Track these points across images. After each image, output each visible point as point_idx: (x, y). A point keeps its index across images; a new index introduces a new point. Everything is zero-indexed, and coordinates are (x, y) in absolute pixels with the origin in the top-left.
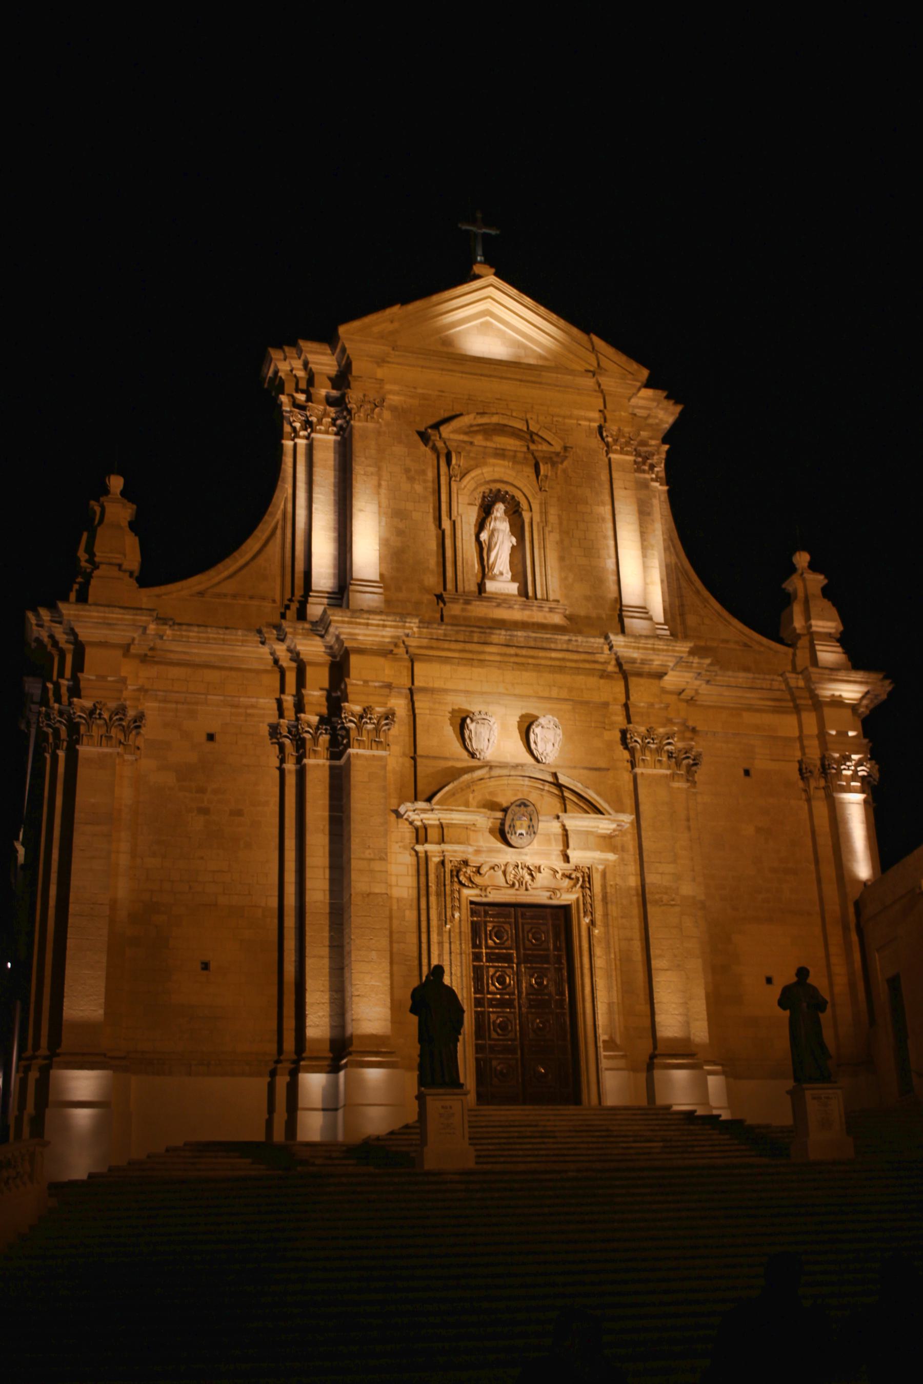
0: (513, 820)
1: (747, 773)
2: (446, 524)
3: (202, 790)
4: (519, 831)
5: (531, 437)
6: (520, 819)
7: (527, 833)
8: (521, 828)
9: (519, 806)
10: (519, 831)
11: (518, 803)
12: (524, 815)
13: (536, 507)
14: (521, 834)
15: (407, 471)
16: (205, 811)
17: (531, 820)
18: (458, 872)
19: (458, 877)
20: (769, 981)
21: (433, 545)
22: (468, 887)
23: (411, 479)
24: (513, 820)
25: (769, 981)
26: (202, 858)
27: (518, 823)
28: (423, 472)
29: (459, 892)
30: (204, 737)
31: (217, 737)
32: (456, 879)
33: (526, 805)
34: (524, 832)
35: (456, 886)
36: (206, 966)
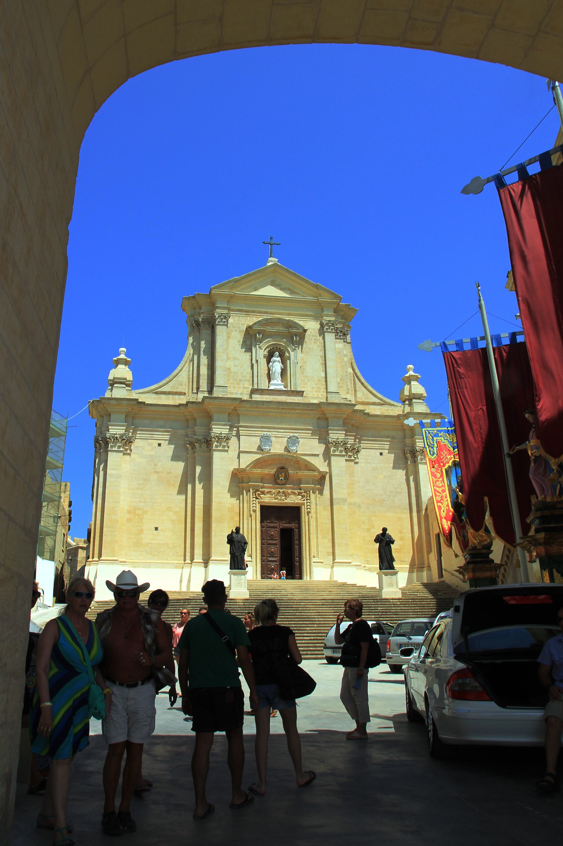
0: (278, 474)
2: (254, 362)
4: (281, 478)
6: (281, 474)
7: (284, 479)
8: (282, 477)
9: (281, 469)
10: (281, 478)
11: (280, 468)
13: (292, 354)
14: (282, 479)
17: (286, 474)
24: (278, 474)
27: (280, 475)
29: (256, 501)
34: (283, 479)
35: (255, 499)
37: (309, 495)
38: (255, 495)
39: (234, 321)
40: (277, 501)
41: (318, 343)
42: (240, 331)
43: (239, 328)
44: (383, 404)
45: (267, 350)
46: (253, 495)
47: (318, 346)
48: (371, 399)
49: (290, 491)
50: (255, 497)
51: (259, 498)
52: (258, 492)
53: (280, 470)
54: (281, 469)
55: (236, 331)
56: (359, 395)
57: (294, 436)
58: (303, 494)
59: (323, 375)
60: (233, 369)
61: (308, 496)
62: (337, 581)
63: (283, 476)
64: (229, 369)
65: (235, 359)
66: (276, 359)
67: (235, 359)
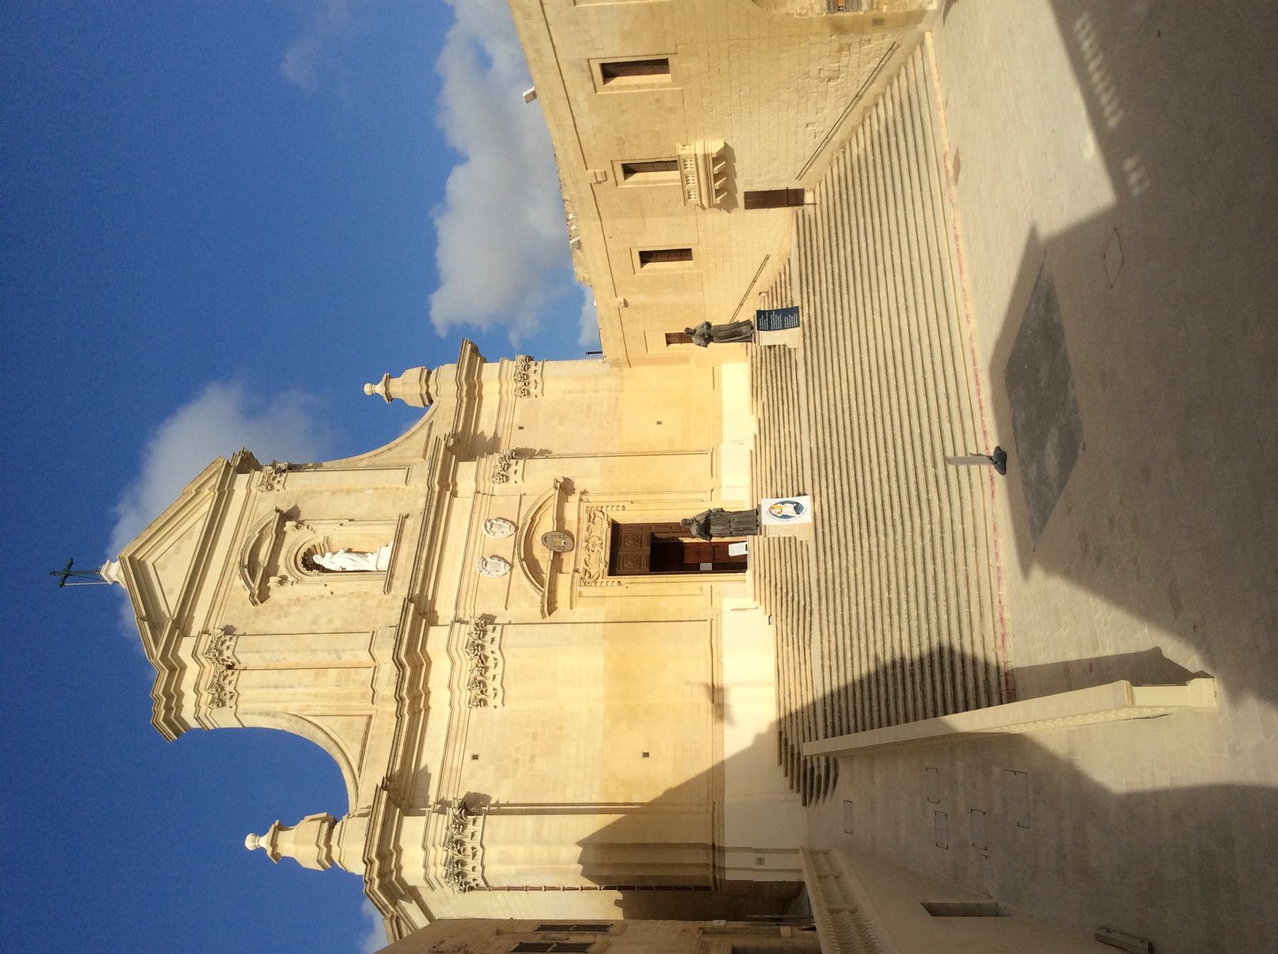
1: (521, 428)
3: (516, 761)
4: (563, 544)
6: (555, 543)
8: (561, 543)
9: (546, 542)
12: (552, 540)
15: (279, 617)
16: (533, 758)
20: (659, 423)
23: (286, 614)
25: (659, 423)
26: (567, 759)
27: (557, 544)
30: (475, 761)
31: (475, 753)
33: (546, 537)
34: (563, 541)
36: (646, 755)
40: (603, 552)
42: (257, 614)
43: (249, 617)
44: (431, 424)
45: (304, 570)
49: (584, 533)
51: (596, 577)
53: (548, 544)
54: (546, 542)
55: (253, 623)
57: (486, 526)
58: (592, 516)
59: (370, 492)
62: (756, 436)
63: (558, 539)
67: (314, 622)
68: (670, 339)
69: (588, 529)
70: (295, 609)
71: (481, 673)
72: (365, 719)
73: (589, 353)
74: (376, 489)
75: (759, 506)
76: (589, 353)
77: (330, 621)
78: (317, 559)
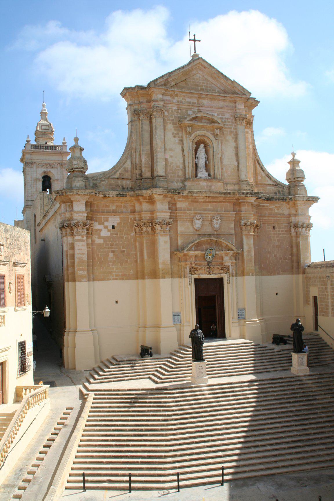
4: (209, 257)
5: (213, 122)
8: (210, 256)
14: (210, 257)
15: (173, 134)
18: (191, 270)
19: (191, 272)
21: (182, 161)
22: (194, 275)
23: (174, 137)
24: (208, 253)
27: (209, 254)
28: (178, 134)
30: (111, 228)
32: (190, 273)
34: (210, 257)
35: (190, 275)
37: (229, 269)
38: (191, 272)
39: (169, 114)
41: (233, 136)
46: (189, 272)
47: (233, 138)
48: (268, 182)
50: (191, 273)
52: (193, 269)
56: (259, 178)
58: (224, 269)
59: (236, 164)
60: (170, 160)
61: (228, 270)
64: (166, 160)
65: (171, 150)
66: (202, 150)
67: (171, 150)
68: (315, 298)
69: (218, 268)
70: (177, 140)
71: (148, 226)
72: (130, 177)
73: (324, 250)
74: (238, 166)
75: (204, 360)
76: (324, 250)
77: (171, 156)
78: (202, 146)
